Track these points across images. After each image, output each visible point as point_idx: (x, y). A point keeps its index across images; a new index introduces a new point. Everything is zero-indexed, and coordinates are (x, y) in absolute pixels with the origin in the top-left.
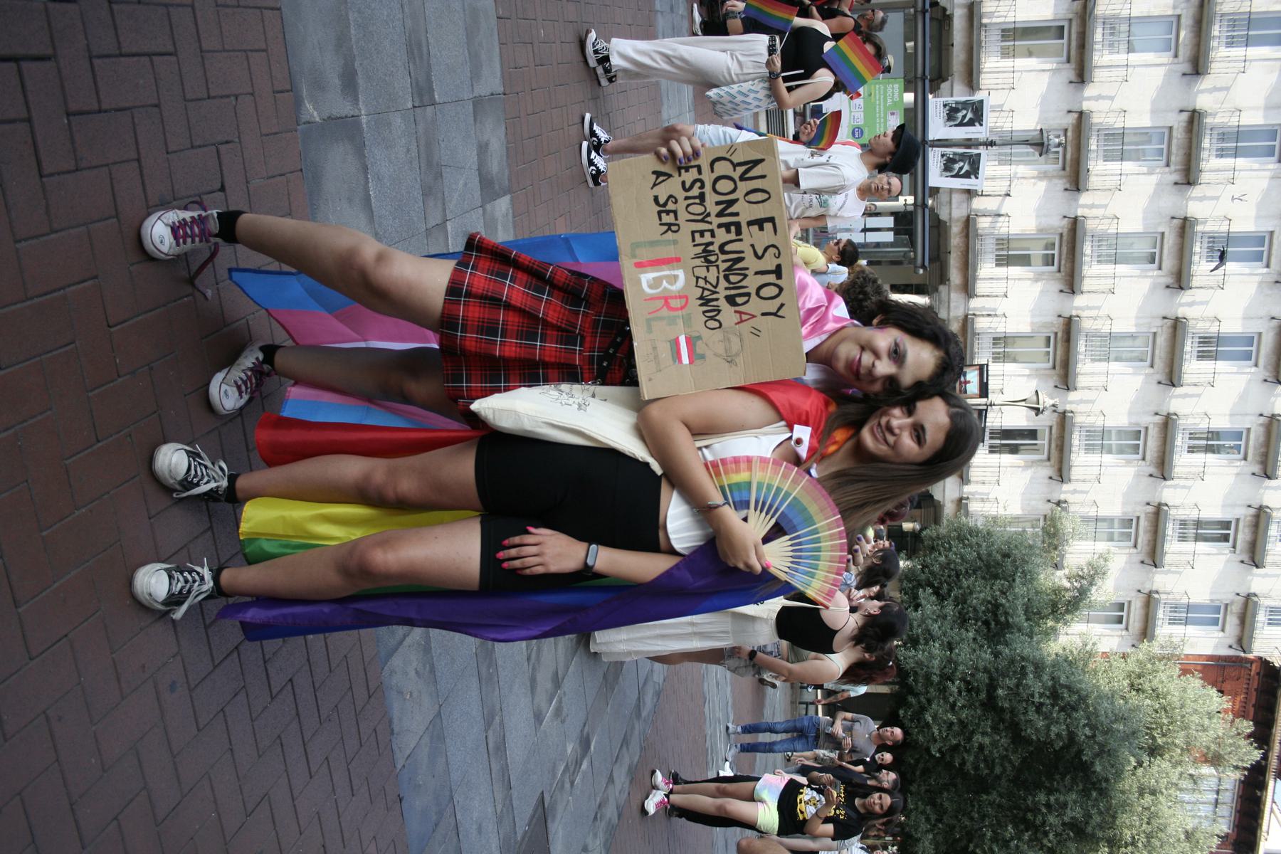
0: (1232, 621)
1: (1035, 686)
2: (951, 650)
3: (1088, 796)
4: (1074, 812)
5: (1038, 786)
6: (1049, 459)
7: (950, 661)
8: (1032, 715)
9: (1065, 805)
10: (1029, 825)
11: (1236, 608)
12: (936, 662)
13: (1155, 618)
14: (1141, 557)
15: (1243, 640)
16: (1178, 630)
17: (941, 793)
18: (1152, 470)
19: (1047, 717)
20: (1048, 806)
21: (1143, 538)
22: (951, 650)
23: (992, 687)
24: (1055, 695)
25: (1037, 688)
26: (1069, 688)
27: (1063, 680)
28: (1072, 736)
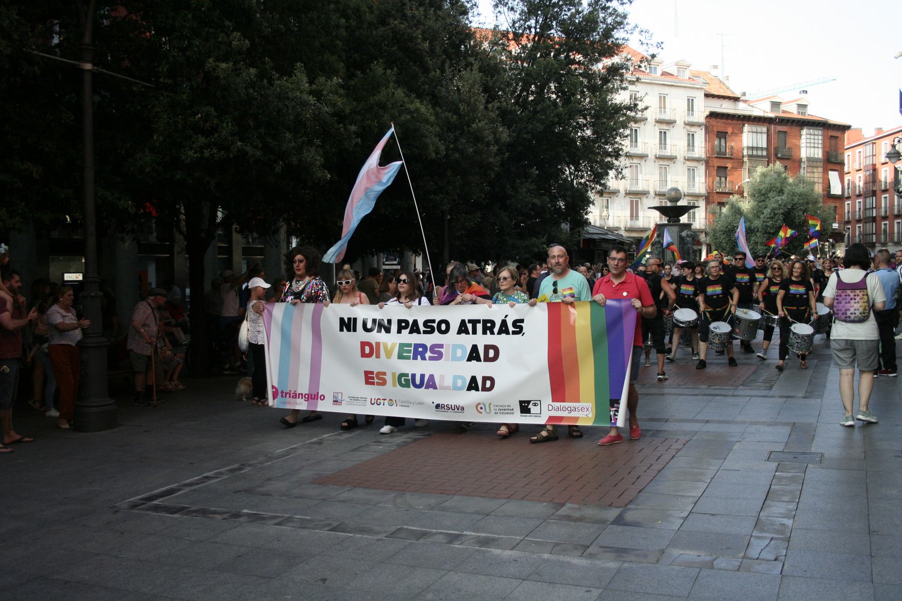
0: (693, 129)
1: (770, 223)
2: (757, 243)
3: (796, 209)
4: (801, 213)
5: (793, 221)
6: (640, 198)
7: (761, 244)
8: (777, 224)
9: (799, 216)
10: (804, 223)
11: (688, 128)
12: (762, 247)
13: (692, 157)
14: (672, 163)
15: (699, 125)
16: (696, 149)
17: (794, 246)
18: (643, 161)
19: (777, 220)
20: (799, 219)
21: (666, 163)
22: (757, 243)
23: (769, 233)
24: (771, 218)
25: (771, 222)
26: (770, 214)
27: (769, 216)
28: (782, 214)
